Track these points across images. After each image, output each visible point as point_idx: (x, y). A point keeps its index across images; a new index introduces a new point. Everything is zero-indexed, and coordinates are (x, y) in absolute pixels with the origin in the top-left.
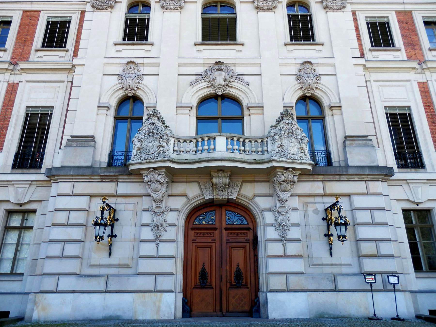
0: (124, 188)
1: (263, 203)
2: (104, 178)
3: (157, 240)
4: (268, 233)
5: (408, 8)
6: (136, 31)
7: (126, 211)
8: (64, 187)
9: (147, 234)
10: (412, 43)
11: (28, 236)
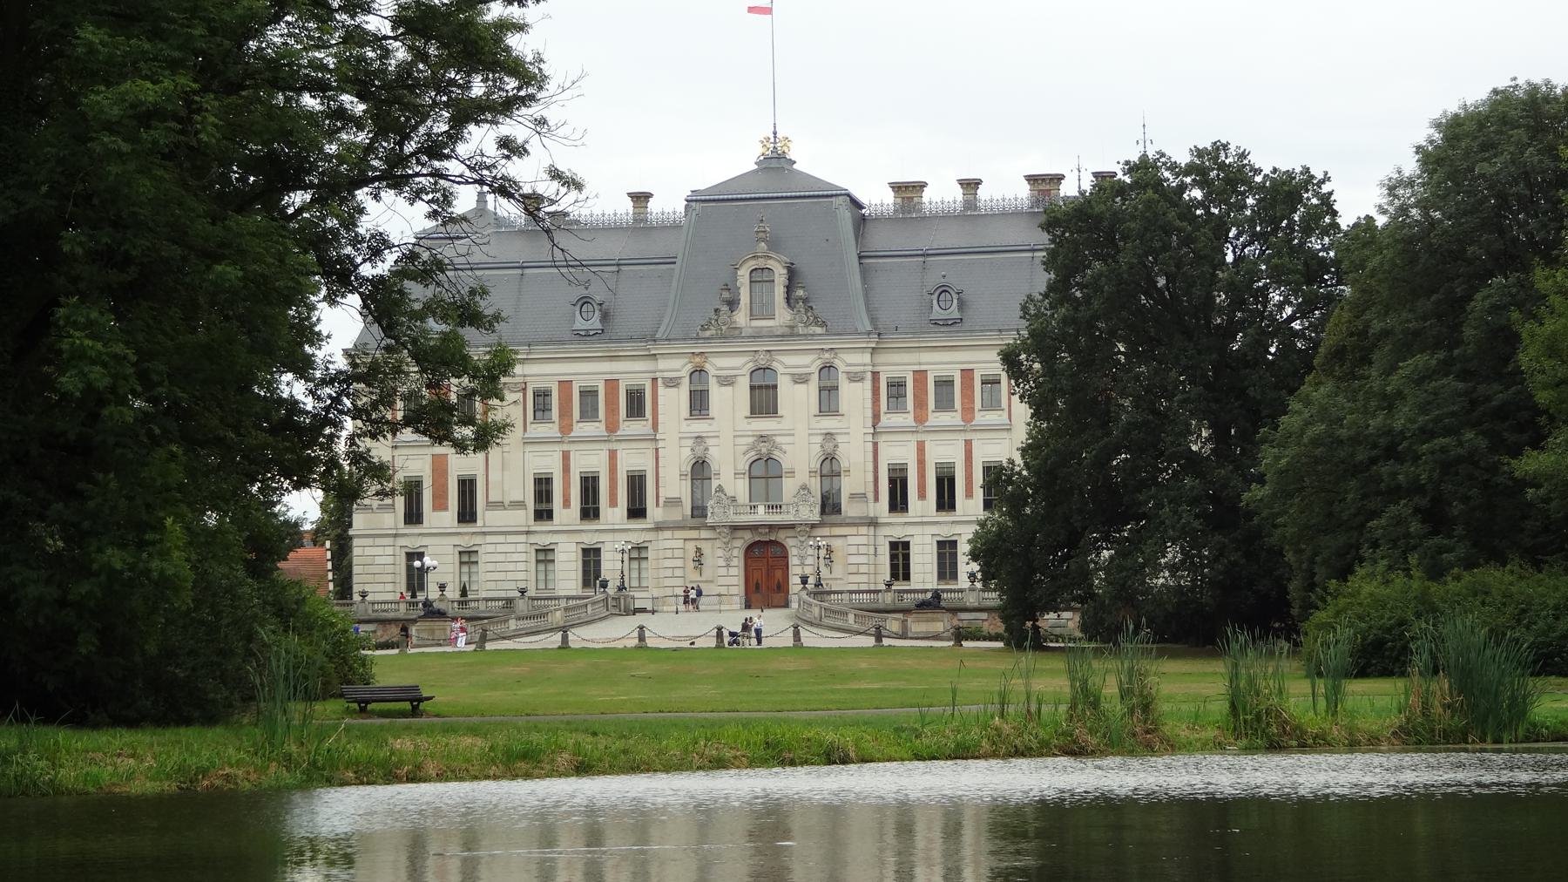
0: (704, 534)
1: (789, 543)
2: (691, 528)
3: (728, 566)
4: (793, 561)
5: (923, 368)
6: (699, 404)
7: (706, 548)
8: (668, 534)
9: (722, 562)
10: (920, 403)
11: (644, 564)
